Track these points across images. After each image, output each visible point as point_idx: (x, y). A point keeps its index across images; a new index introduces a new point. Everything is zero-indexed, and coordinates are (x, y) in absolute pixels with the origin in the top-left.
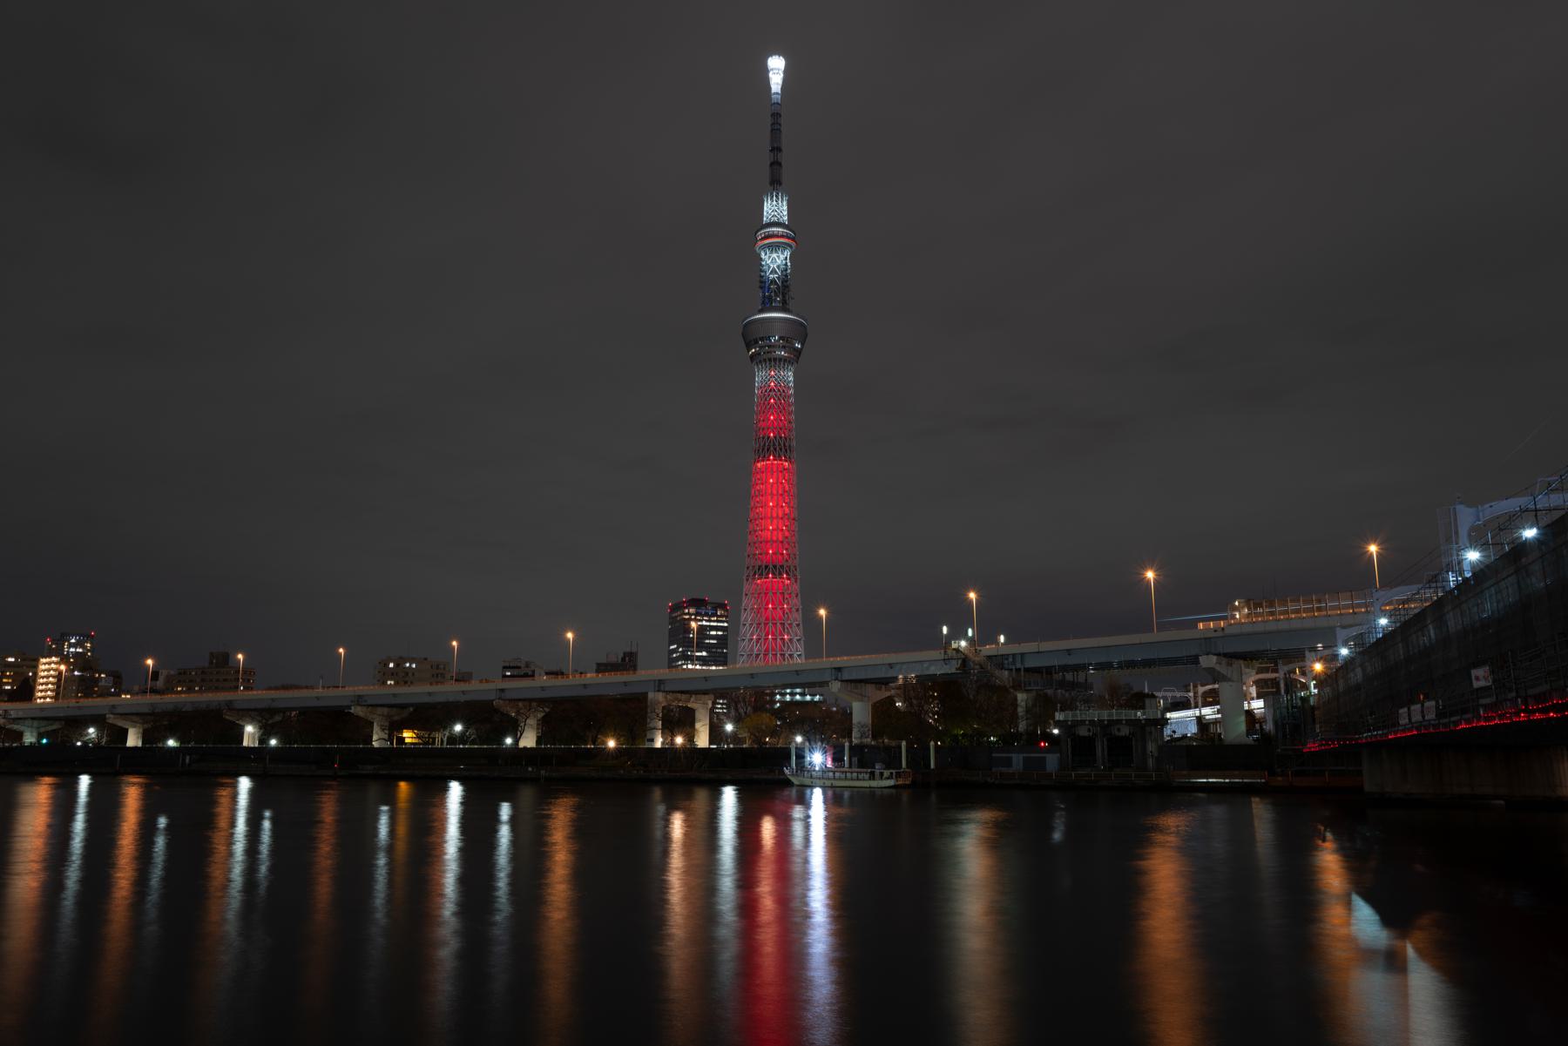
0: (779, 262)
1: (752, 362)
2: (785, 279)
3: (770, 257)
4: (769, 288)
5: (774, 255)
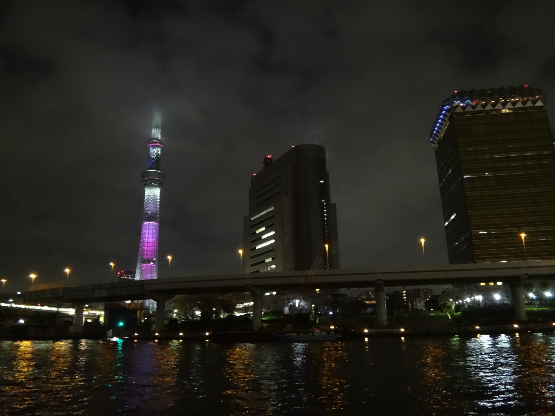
0: (156, 152)
1: (145, 186)
3: (152, 150)
5: (154, 150)
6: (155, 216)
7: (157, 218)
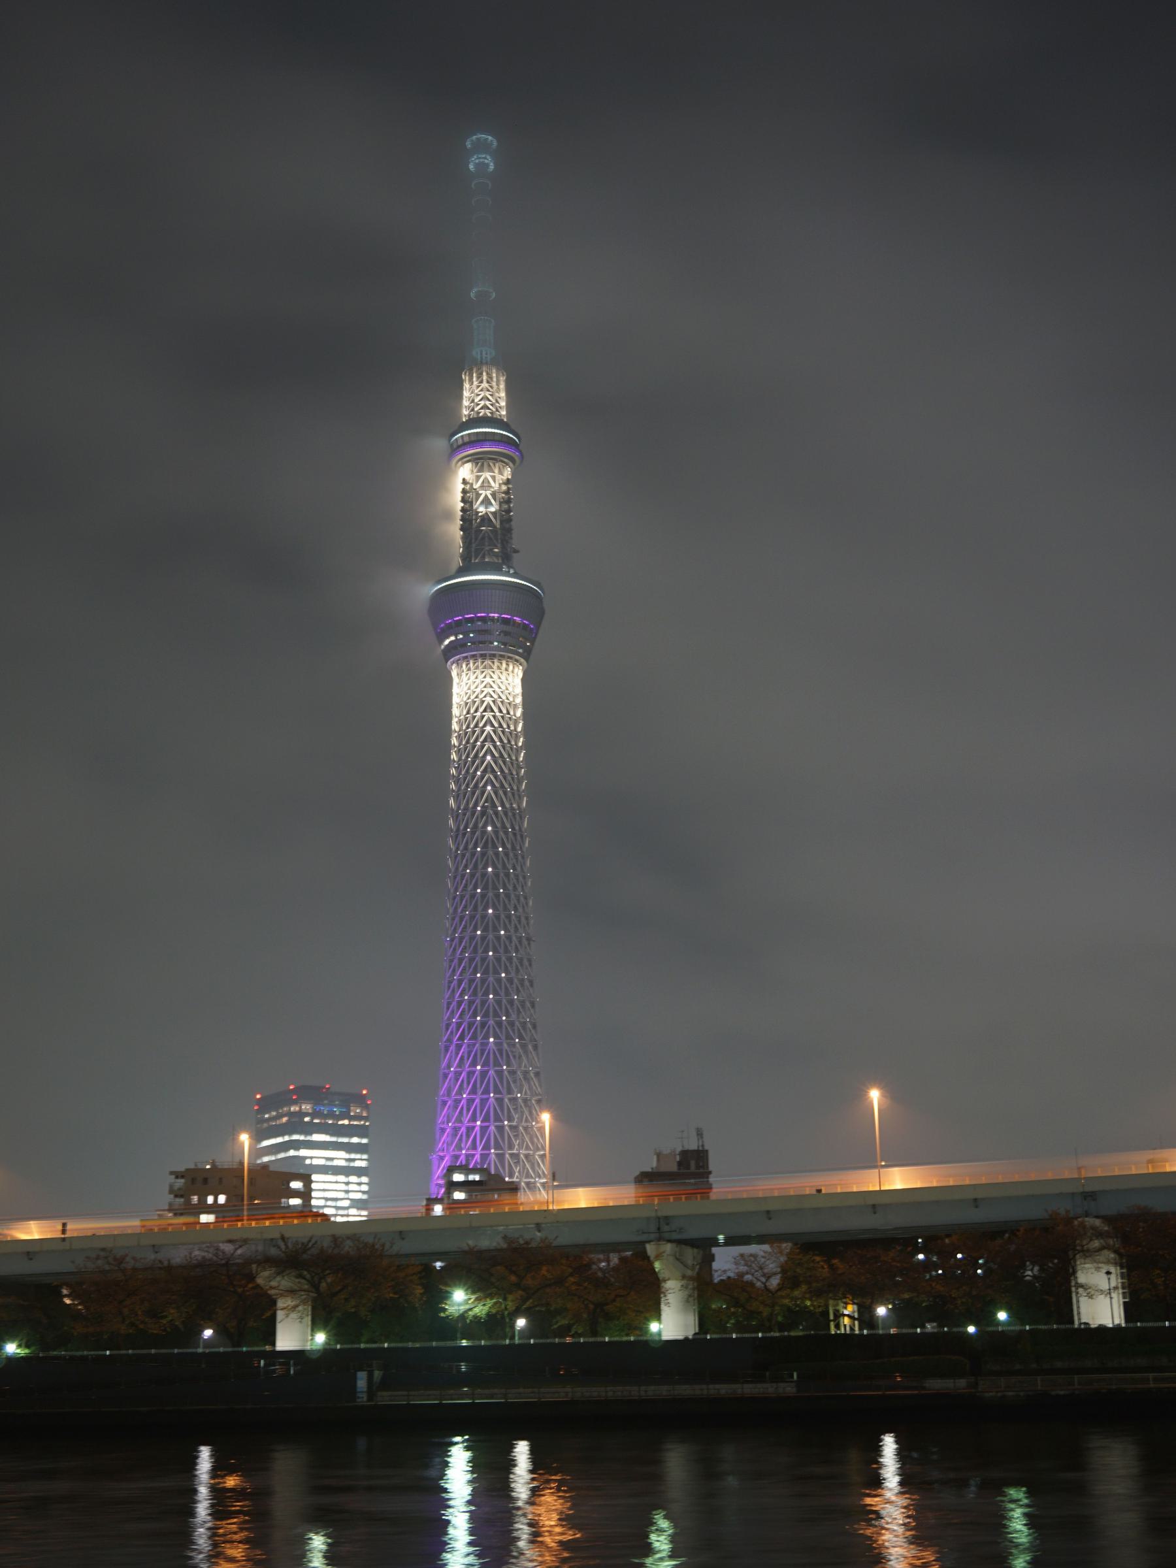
0: (495, 486)
1: (447, 662)
2: (505, 515)
3: (478, 478)
5: (487, 475)
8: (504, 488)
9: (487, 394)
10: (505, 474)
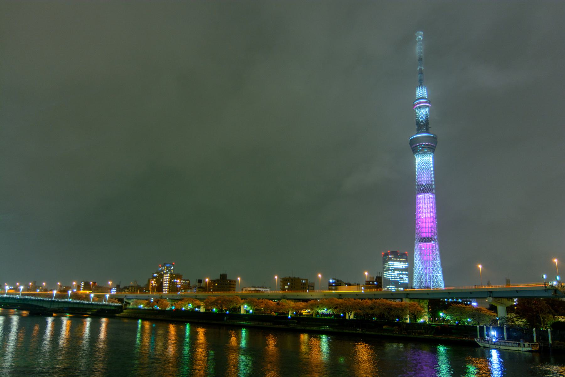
0: (424, 113)
1: (414, 154)
2: (427, 120)
3: (420, 112)
4: (420, 124)
5: (422, 111)
6: (431, 187)
7: (432, 189)
8: (426, 113)
9: (421, 92)
10: (426, 110)
